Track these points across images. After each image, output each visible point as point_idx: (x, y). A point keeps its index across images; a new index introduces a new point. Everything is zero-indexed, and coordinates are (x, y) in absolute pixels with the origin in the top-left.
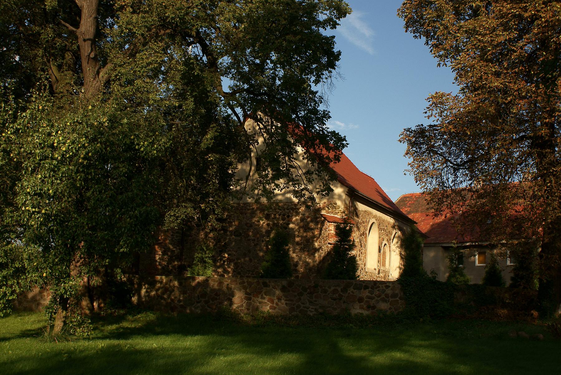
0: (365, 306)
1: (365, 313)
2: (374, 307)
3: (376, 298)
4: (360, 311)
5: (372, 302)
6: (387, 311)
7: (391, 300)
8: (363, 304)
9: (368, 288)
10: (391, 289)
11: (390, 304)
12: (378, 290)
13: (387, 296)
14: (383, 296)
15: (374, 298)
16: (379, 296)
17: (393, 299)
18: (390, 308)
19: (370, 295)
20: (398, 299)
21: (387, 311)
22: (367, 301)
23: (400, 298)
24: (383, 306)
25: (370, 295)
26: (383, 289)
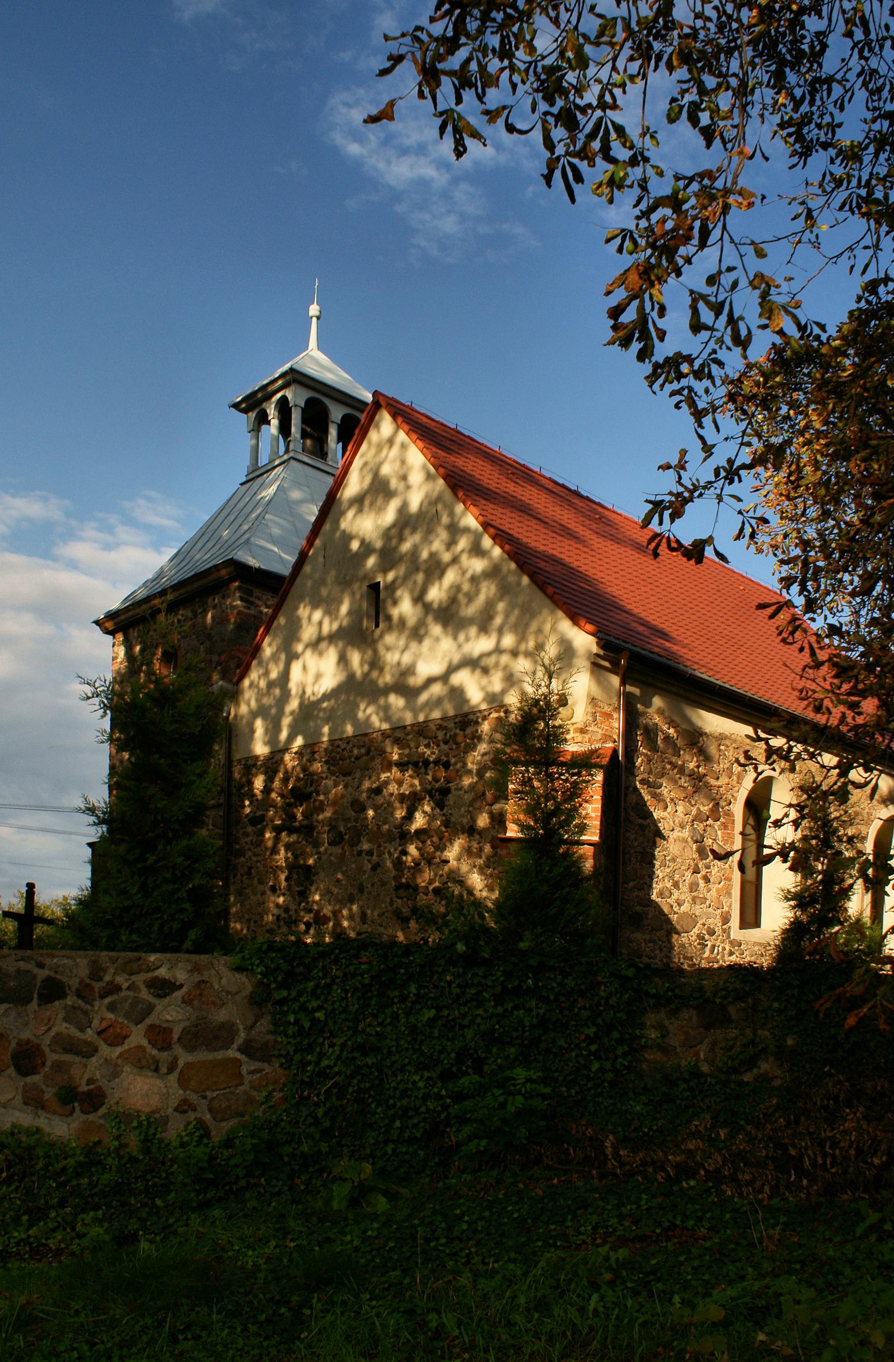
0: (49, 1094)
1: (61, 1128)
2: (93, 1100)
3: (105, 1051)
4: (25, 1119)
5: (86, 1073)
6: (165, 1121)
7: (185, 1058)
8: (35, 1079)
9: (62, 995)
10: (187, 1001)
11: (183, 1082)
12: (111, 1008)
13: (160, 1036)
14: (137, 1037)
15: (94, 1050)
16: (118, 1040)
17: (203, 1056)
18: (184, 1107)
19: (74, 1031)
20: (233, 1053)
21: (165, 1121)
22: (59, 1067)
23: (246, 1049)
24: (141, 1091)
25: (74, 1031)
26: (136, 1001)
